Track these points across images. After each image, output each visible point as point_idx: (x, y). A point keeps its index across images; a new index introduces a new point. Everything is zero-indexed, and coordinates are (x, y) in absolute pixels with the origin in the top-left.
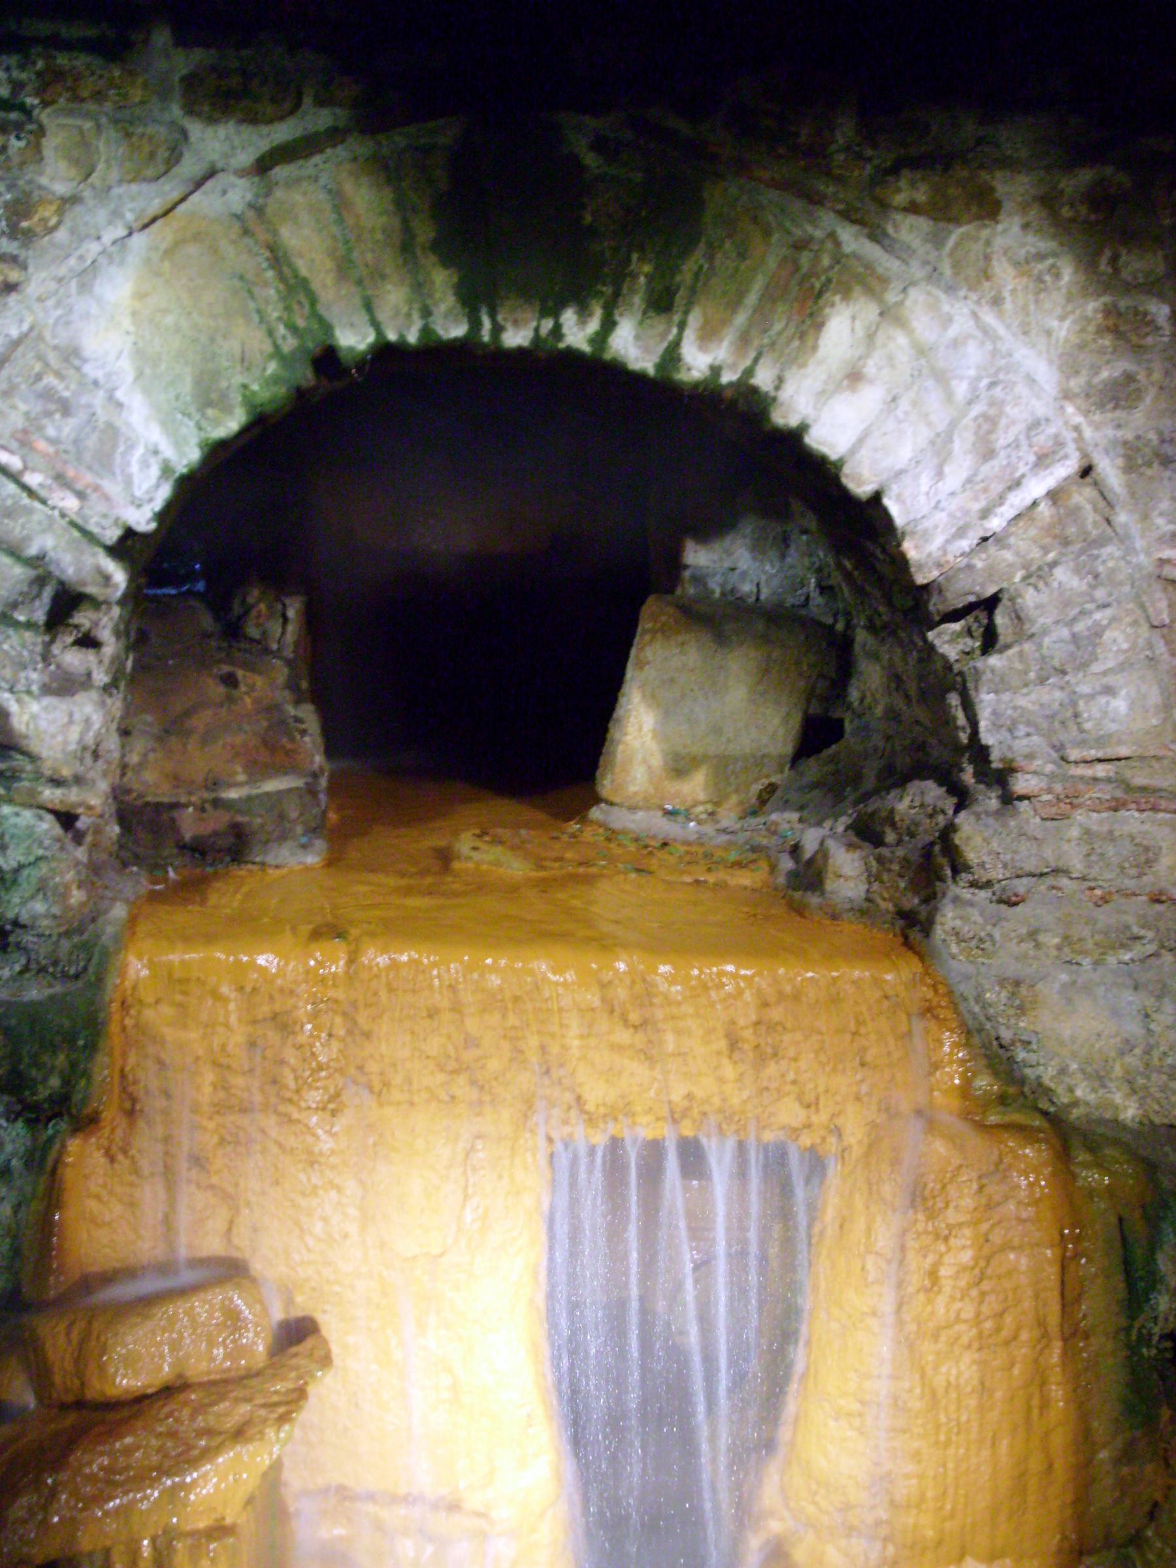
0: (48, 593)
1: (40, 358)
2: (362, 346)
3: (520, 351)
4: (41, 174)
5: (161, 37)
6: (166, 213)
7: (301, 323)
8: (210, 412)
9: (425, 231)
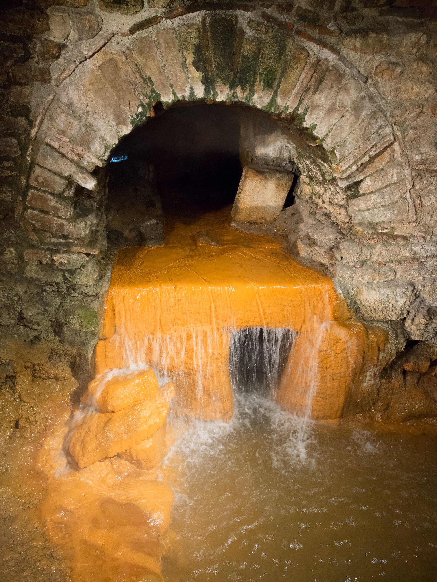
1: (60, 107)
2: (170, 101)
3: (222, 102)
4: (50, 35)
6: (98, 52)
8: (120, 126)
9: (190, 59)
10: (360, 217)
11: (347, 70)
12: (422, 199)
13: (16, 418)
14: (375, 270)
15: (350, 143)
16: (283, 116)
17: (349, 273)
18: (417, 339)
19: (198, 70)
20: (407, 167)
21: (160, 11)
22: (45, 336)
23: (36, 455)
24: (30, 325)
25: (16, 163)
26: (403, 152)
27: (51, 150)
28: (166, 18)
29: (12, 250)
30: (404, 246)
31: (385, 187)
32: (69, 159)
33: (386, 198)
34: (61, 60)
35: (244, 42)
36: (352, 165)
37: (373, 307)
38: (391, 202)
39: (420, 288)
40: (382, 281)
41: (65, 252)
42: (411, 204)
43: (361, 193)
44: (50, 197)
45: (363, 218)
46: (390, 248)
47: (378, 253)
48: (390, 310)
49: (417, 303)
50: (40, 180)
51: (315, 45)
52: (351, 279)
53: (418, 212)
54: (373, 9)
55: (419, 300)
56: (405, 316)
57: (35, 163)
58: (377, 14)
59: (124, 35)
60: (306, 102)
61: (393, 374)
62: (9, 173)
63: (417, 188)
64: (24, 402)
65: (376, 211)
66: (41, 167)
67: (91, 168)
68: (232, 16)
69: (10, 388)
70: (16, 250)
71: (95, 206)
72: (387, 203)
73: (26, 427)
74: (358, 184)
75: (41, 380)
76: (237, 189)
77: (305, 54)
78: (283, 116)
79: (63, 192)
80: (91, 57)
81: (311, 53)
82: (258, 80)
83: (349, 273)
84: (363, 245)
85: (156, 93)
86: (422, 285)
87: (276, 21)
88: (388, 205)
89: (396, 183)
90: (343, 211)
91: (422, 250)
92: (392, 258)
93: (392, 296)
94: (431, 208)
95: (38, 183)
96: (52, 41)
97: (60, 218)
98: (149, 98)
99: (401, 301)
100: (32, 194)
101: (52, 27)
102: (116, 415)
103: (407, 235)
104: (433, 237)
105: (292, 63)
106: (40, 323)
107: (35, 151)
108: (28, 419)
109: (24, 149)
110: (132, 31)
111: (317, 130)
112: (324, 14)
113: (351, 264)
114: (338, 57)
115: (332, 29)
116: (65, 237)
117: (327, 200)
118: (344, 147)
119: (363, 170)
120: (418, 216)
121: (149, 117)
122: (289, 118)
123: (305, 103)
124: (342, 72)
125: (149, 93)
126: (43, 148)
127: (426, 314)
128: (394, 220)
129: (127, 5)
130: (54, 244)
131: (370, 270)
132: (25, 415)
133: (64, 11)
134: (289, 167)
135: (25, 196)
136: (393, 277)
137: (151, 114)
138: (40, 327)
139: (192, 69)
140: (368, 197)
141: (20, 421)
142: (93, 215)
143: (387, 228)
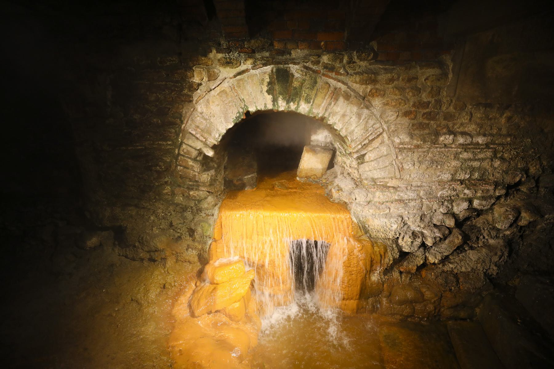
0: (202, 155)
2: (254, 111)
3: (282, 111)
5: (214, 51)
7: (243, 106)
9: (265, 88)
10: (366, 175)
11: (352, 93)
12: (403, 165)
13: (164, 282)
14: (376, 206)
15: (356, 133)
16: (317, 118)
17: (360, 208)
18: (407, 251)
19: (269, 94)
20: (392, 146)
21: (250, 66)
22: (184, 237)
23: (173, 305)
24: (176, 230)
25: (173, 142)
26: (389, 138)
27: (191, 135)
28: (253, 69)
29: (169, 187)
30: (394, 193)
31: (380, 158)
32: (200, 140)
33: (380, 164)
34: (199, 91)
35: (294, 80)
36: (358, 145)
37: (377, 230)
38: (383, 166)
39: (407, 219)
40: (382, 214)
41: (196, 189)
42: (396, 168)
43: (365, 161)
44: (189, 160)
45: (367, 175)
46: (385, 194)
47: (378, 197)
48: (388, 232)
49: (405, 228)
50: (185, 151)
51: (333, 80)
52: (361, 212)
53: (401, 172)
54: (366, 62)
55: (406, 226)
56: (398, 236)
57: (183, 142)
58: (368, 64)
59: (231, 78)
60: (329, 110)
61: (393, 273)
62: (168, 147)
63: (399, 159)
64: (170, 274)
65: (375, 172)
66: (186, 144)
67: (211, 145)
68: (287, 68)
69: (163, 265)
70: (170, 188)
71: (216, 166)
72: (381, 167)
73: (169, 288)
74: (364, 155)
75: (181, 262)
76: (300, 159)
77: (328, 85)
78: (317, 118)
79: (197, 157)
80: (214, 89)
81: (331, 85)
82: (302, 99)
83: (360, 208)
84: (368, 192)
85: (246, 106)
86: (407, 217)
87: (311, 69)
88: (382, 168)
89: (387, 155)
90: (356, 171)
91: (406, 195)
92: (387, 200)
93: (388, 224)
94: (409, 170)
95: (184, 152)
96: (195, 82)
97: (194, 171)
98: (243, 109)
99: (395, 227)
100: (181, 158)
101: (195, 76)
102: (218, 286)
103: (396, 186)
104: (412, 188)
105: (321, 90)
106: (181, 229)
107: (184, 137)
108: (170, 284)
109: (178, 135)
110: (235, 76)
111: (336, 125)
112: (337, 65)
113: (361, 203)
114: (346, 87)
115: (342, 72)
116: (197, 181)
117: (348, 165)
118: (353, 135)
119: (366, 148)
120: (401, 175)
121: (243, 119)
122: (320, 119)
123: (329, 111)
124: (349, 94)
125: (243, 106)
126: (187, 135)
127: (411, 235)
128: (386, 177)
129: (233, 64)
130: (191, 185)
131: (374, 207)
132: (169, 281)
133: (201, 68)
134: (331, 147)
135: (177, 159)
136: (388, 212)
137: (243, 117)
138: (181, 231)
139: (266, 94)
140: (370, 163)
141: (166, 284)
142: (214, 170)
143: (382, 182)
